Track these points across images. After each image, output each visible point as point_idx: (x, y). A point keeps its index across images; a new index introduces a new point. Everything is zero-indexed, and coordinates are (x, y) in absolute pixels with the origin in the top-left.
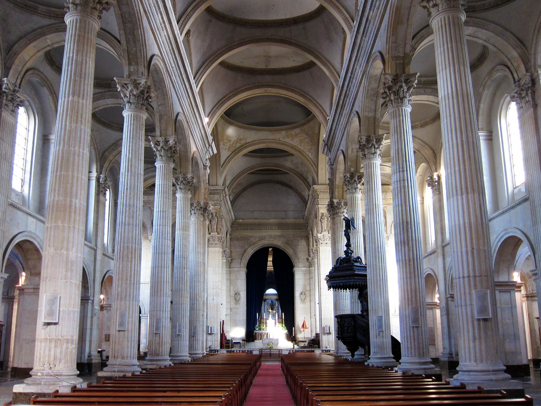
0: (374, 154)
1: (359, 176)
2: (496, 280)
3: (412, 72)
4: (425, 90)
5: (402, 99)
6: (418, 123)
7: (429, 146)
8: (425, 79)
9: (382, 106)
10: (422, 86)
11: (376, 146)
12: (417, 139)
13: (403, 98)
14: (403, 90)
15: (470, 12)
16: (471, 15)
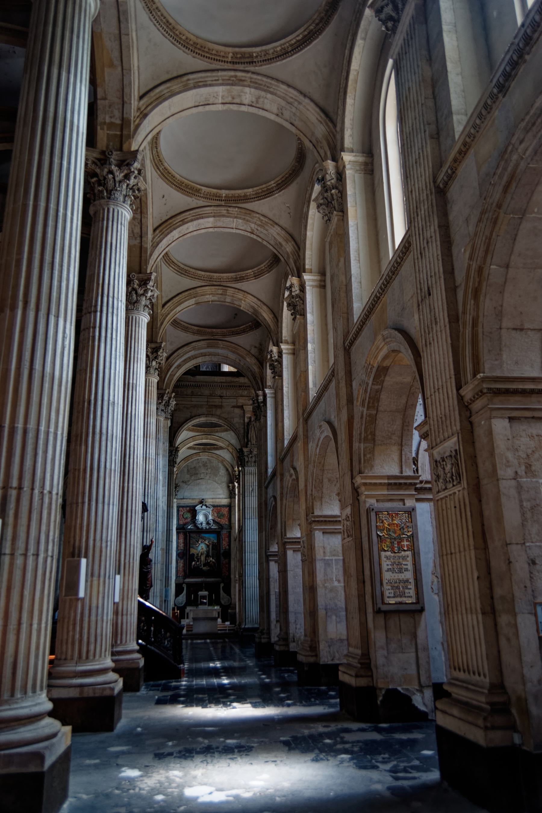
0: (134, 303)
1: (154, 349)
2: (317, 512)
3: (134, 148)
4: (228, 210)
5: (110, 192)
6: (251, 271)
7: (268, 306)
8: (227, 192)
9: (155, 230)
10: (223, 203)
11: (141, 291)
12: (251, 296)
13: (112, 190)
14: (114, 178)
15: (244, 63)
16: (246, 69)
